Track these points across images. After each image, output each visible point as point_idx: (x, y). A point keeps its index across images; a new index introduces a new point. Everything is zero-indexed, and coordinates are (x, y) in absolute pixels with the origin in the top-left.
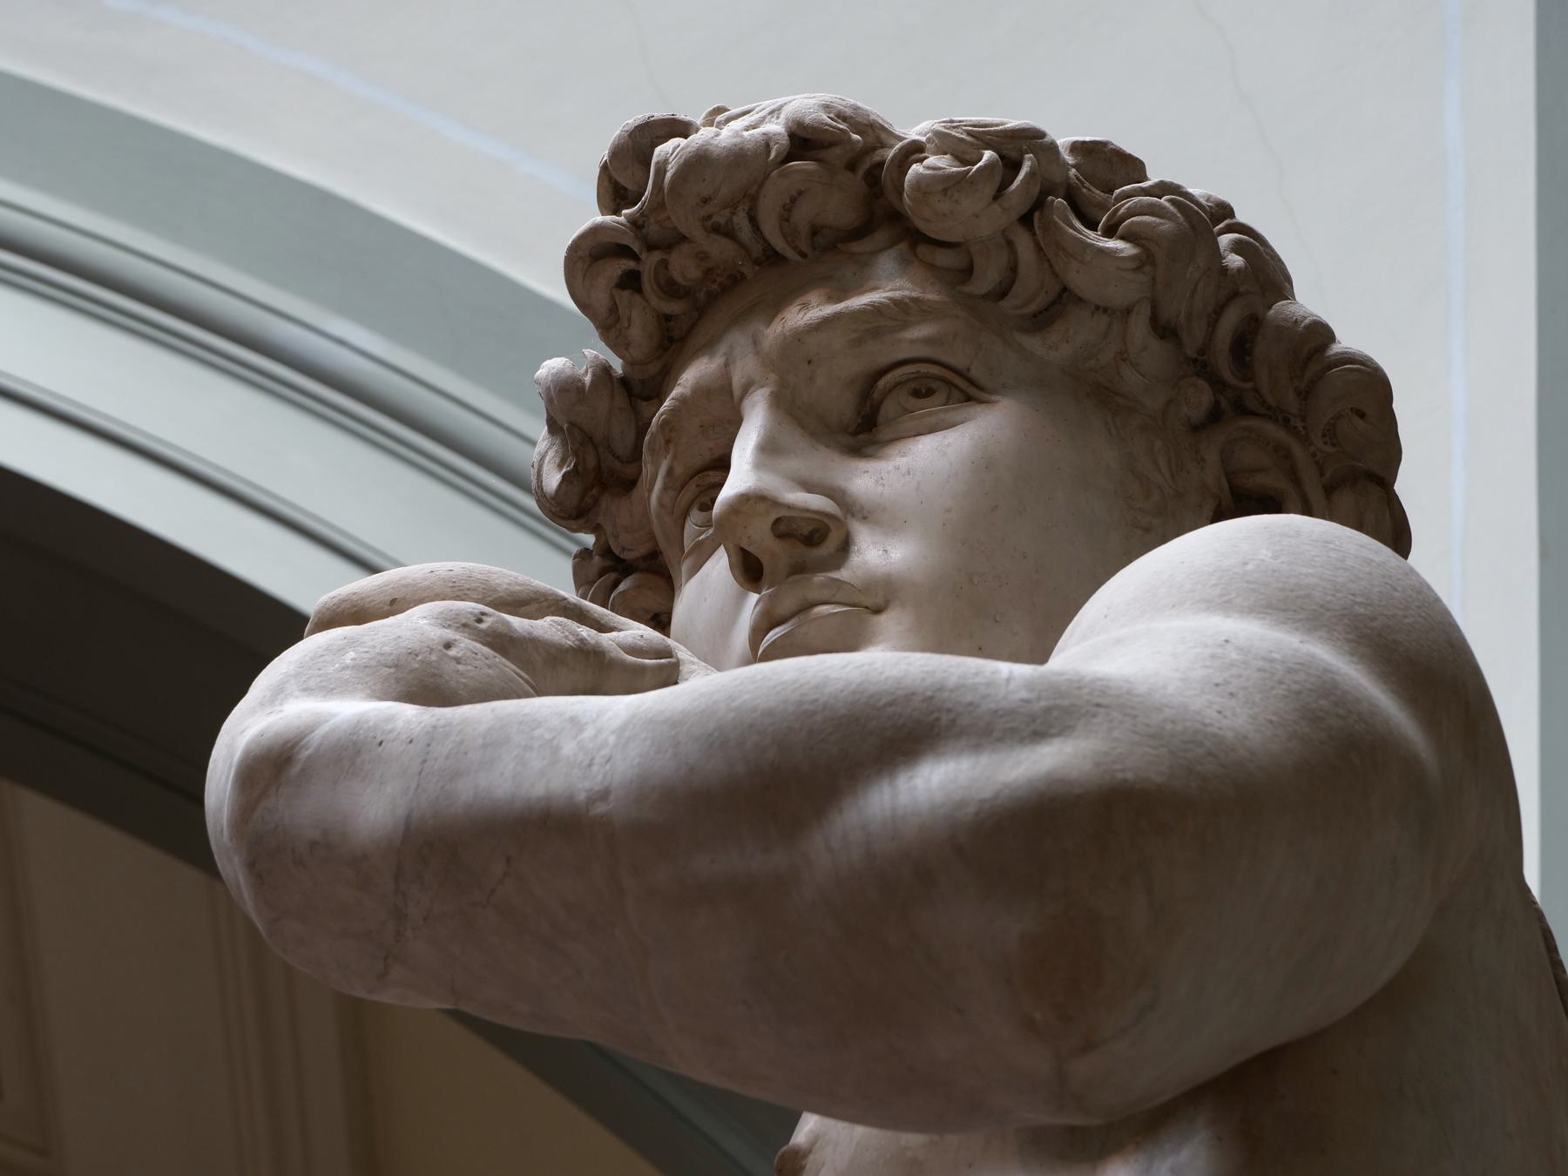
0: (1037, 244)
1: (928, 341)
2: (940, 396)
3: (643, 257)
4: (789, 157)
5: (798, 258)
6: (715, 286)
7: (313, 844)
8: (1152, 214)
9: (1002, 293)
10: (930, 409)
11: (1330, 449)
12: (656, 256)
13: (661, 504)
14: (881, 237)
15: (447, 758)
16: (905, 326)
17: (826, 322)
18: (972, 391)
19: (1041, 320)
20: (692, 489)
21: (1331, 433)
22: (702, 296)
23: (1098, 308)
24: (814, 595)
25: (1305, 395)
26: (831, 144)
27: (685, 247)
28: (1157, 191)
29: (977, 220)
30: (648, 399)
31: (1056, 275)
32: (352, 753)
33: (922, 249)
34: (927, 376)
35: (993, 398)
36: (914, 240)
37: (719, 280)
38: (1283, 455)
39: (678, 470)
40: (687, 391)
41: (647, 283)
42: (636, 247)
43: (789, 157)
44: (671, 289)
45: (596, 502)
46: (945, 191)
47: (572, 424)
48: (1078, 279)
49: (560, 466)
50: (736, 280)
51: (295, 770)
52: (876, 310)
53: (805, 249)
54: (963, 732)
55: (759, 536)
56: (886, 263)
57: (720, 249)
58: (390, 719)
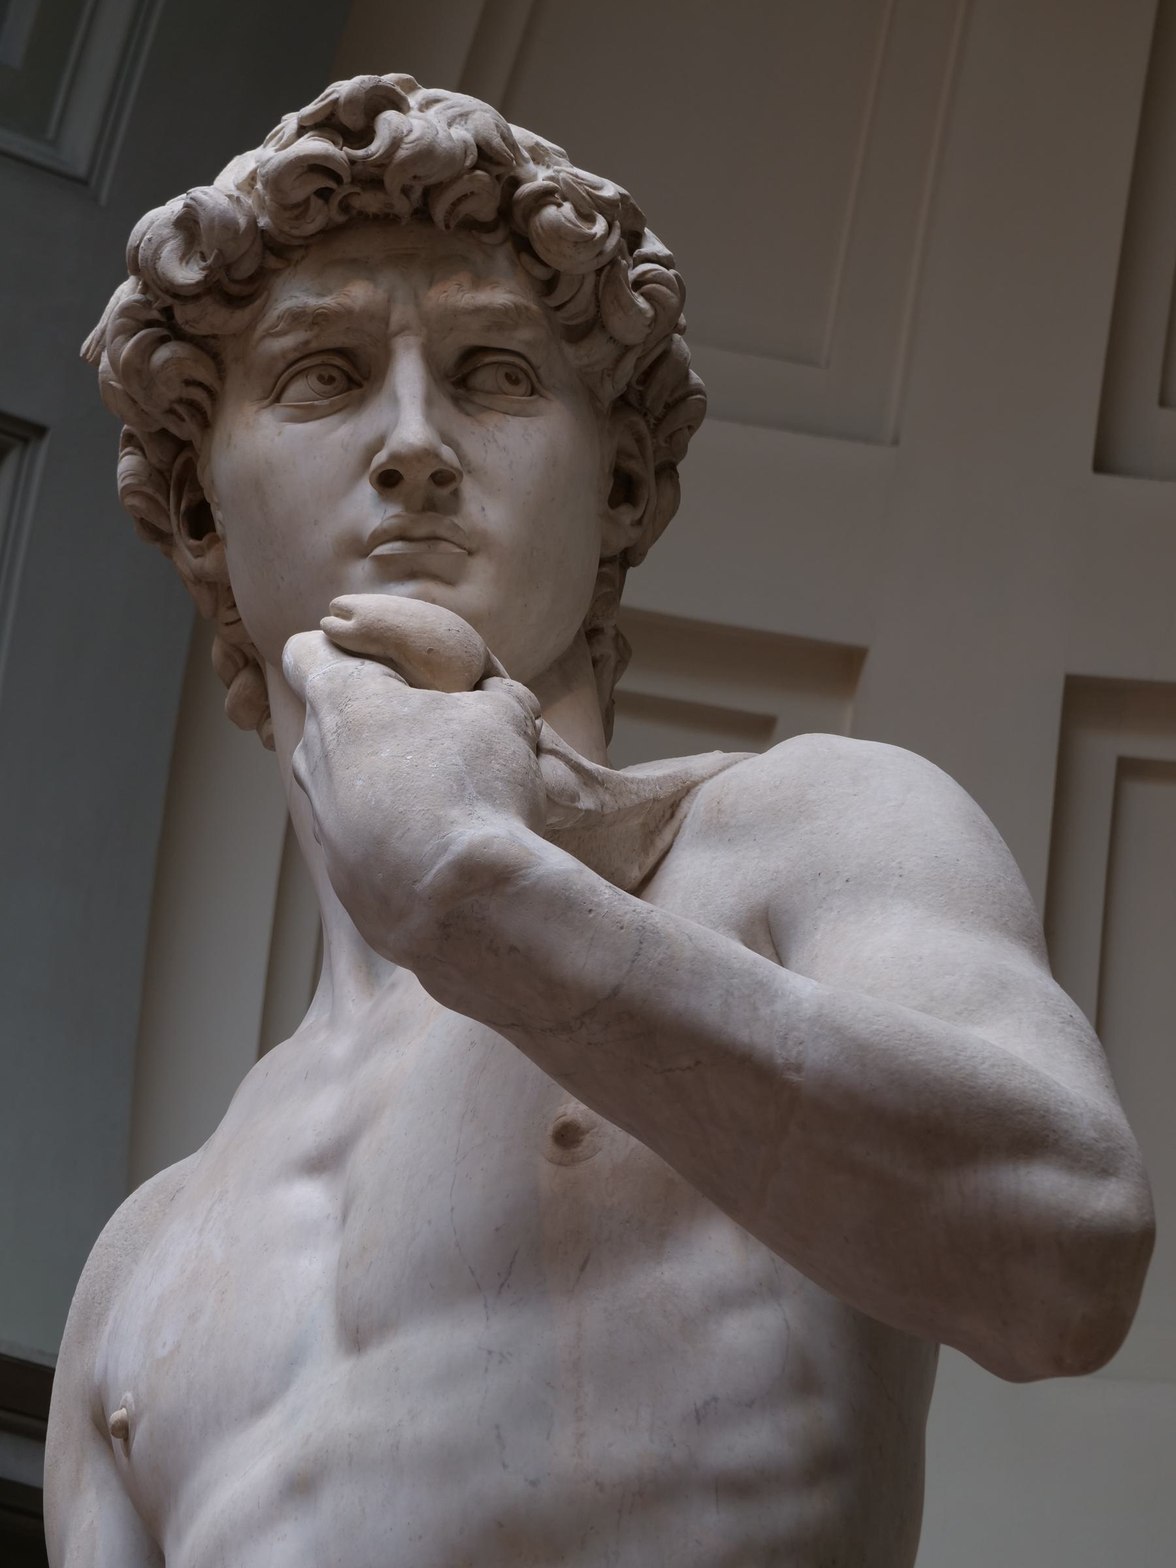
0: (596, 286)
2: (524, 387)
4: (475, 167)
5: (443, 228)
7: (513, 949)
8: (667, 287)
11: (663, 444)
12: (357, 189)
13: (284, 354)
14: (500, 234)
15: (660, 964)
17: (478, 311)
18: (537, 385)
19: (577, 334)
20: (317, 360)
21: (671, 436)
22: (354, 212)
23: (611, 338)
24: (441, 532)
25: (670, 407)
26: (499, 164)
28: (665, 261)
30: (271, 249)
31: (599, 307)
32: (562, 904)
33: (525, 258)
34: (522, 369)
36: (523, 245)
38: (639, 440)
39: (314, 346)
41: (335, 201)
42: (346, 178)
44: (345, 207)
45: (196, 297)
46: (576, 243)
47: (221, 253)
48: (617, 323)
49: (181, 259)
50: (387, 220)
52: (505, 311)
53: (453, 224)
55: (417, 477)
56: (502, 258)
57: (402, 206)
58: (593, 890)
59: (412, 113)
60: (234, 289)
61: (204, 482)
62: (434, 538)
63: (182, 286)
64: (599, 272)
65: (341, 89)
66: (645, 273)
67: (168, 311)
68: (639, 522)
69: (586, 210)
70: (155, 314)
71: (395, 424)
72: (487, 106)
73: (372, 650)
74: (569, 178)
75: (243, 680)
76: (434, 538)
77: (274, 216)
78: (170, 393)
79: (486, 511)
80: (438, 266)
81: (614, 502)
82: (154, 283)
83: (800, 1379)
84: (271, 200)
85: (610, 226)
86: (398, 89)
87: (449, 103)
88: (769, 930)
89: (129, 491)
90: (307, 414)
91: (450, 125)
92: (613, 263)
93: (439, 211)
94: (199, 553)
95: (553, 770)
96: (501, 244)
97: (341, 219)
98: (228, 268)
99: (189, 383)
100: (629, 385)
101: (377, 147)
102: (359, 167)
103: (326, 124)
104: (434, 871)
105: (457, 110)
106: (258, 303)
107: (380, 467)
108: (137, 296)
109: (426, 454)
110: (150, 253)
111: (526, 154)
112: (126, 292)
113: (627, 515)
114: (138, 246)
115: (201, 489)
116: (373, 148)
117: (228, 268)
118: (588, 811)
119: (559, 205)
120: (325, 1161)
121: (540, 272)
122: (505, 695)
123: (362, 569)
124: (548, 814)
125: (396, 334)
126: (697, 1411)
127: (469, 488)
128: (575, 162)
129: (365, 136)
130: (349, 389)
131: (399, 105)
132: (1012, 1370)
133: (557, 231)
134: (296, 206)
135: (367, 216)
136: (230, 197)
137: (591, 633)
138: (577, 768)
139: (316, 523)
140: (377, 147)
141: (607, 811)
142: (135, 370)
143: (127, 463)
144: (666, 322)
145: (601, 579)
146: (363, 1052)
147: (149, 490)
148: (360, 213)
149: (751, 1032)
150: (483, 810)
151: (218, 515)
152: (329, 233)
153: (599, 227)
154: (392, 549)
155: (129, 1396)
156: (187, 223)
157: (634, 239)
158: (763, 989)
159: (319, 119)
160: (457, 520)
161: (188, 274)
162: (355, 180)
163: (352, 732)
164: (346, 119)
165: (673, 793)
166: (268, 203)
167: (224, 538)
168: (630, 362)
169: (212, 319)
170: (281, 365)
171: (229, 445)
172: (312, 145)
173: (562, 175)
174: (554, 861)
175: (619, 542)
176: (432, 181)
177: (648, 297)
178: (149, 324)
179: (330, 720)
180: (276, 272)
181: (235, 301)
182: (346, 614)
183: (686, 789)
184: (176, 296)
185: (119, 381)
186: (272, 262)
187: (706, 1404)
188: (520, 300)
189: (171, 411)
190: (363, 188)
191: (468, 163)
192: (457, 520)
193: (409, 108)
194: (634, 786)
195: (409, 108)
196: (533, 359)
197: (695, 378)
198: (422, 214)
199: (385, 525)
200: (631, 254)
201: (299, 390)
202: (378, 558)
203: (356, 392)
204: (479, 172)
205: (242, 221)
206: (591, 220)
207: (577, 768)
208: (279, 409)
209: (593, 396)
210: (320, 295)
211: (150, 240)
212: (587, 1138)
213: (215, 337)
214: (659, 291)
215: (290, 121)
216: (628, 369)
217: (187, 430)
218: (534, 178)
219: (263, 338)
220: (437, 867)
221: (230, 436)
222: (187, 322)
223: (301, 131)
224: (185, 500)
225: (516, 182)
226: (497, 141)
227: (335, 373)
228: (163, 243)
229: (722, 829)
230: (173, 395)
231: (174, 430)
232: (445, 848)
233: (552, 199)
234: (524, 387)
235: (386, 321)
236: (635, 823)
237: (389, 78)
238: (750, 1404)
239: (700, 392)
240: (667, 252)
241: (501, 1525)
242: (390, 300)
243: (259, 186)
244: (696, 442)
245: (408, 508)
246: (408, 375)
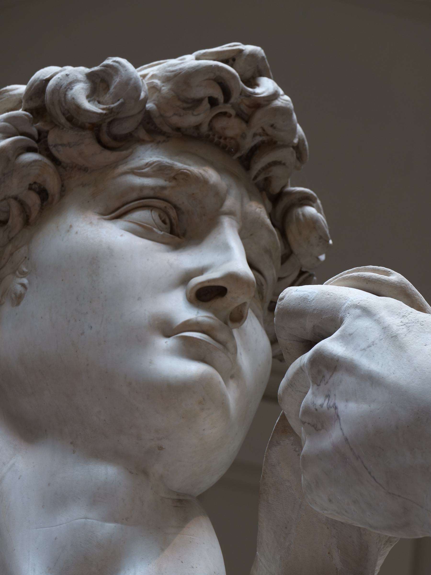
3: (229, 105)
5: (253, 177)
6: (216, 139)
12: (232, 112)
13: (142, 188)
27: (244, 125)
37: (222, 141)
39: (166, 193)
42: (232, 100)
45: (82, 127)
46: (321, 238)
49: (88, 97)
60: (106, 138)
70: (34, 130)
71: (229, 260)
78: (16, 186)
84: (171, 89)
90: (144, 232)
99: (30, 188)
106: (124, 153)
110: (65, 83)
114: (48, 80)
123: (165, 343)
133: (313, 222)
134: (185, 101)
139: (139, 299)
154: (201, 337)
170: (134, 195)
171: (68, 231)
180: (142, 142)
186: (142, 134)
203: (177, 238)
205: (143, 95)
208: (121, 223)
211: (67, 75)
221: (71, 226)
222: (55, 146)
227: (167, 221)
228: (76, 81)
233: (311, 203)
235: (222, 201)
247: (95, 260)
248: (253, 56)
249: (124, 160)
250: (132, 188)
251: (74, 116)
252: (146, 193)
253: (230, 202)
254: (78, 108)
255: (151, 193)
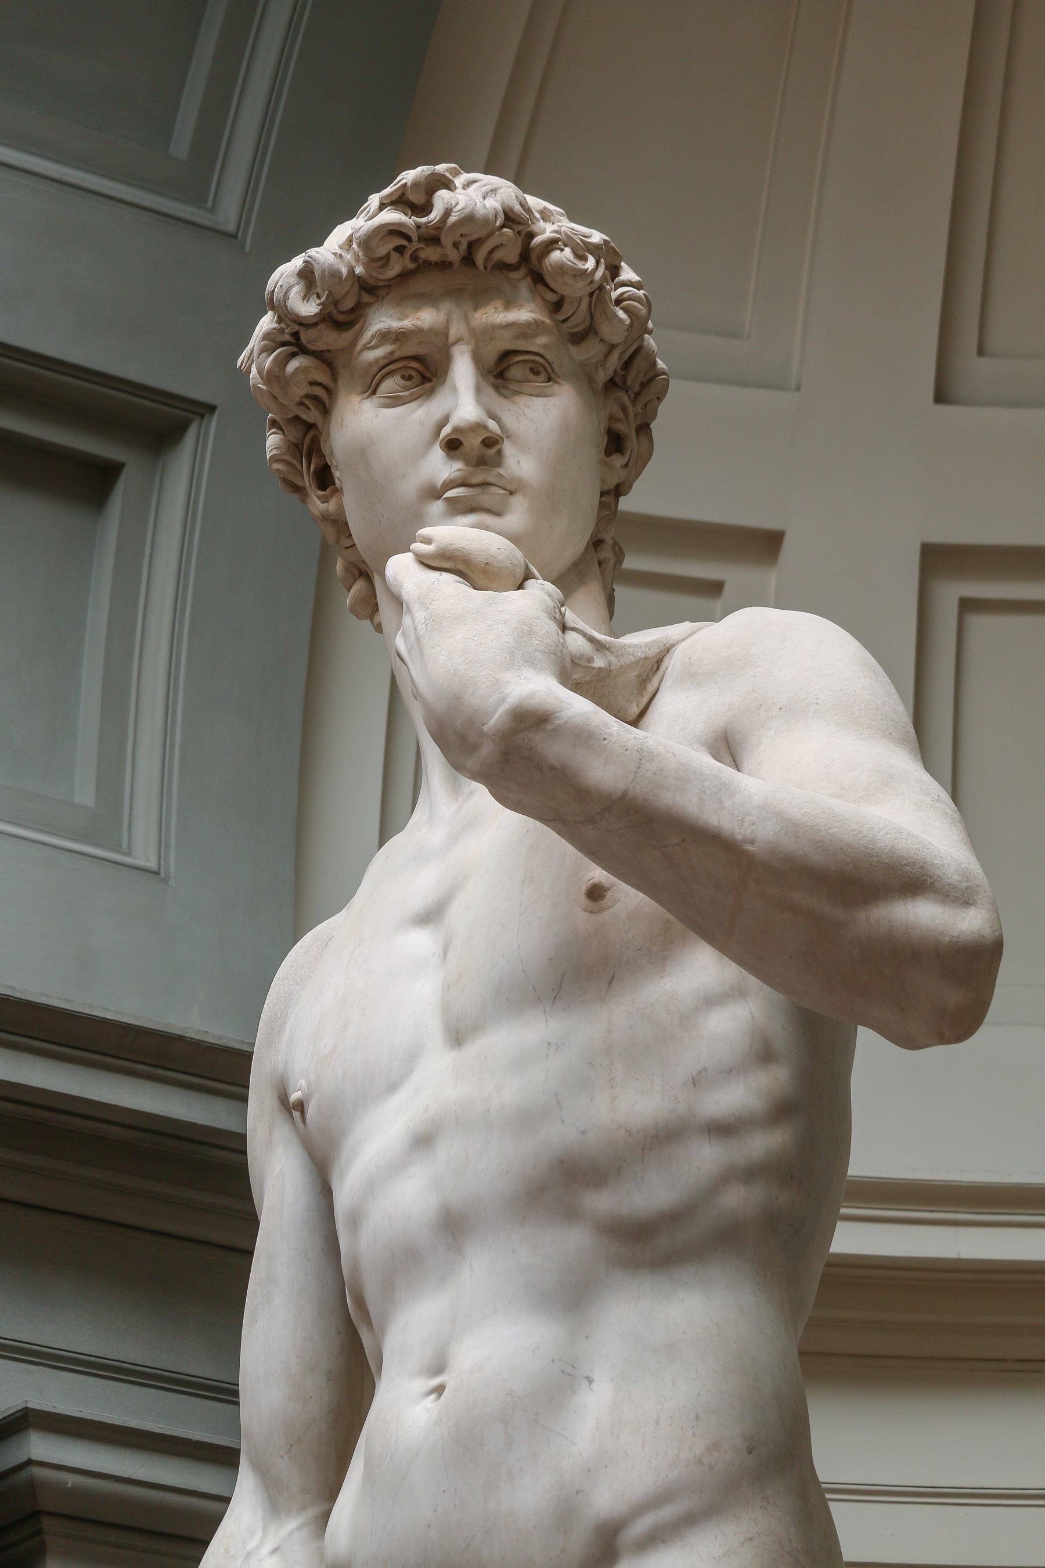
0: (590, 304)
1: (545, 346)
2: (543, 376)
4: (503, 226)
7: (552, 768)
8: (639, 302)
9: (564, 321)
10: (539, 384)
11: (640, 411)
12: (422, 245)
13: (377, 361)
14: (522, 272)
16: (535, 336)
17: (509, 325)
18: (553, 375)
19: (577, 339)
24: (491, 479)
25: (645, 385)
26: (519, 223)
27: (439, 250)
29: (577, 290)
32: (584, 736)
33: (540, 287)
34: (541, 364)
35: (562, 382)
36: (538, 279)
38: (624, 409)
39: (398, 355)
40: (426, 328)
41: (408, 254)
42: (415, 238)
43: (503, 226)
44: (414, 258)
45: (315, 324)
46: (574, 276)
47: (330, 292)
48: (605, 330)
49: (304, 299)
51: (549, 727)
52: (528, 324)
54: (936, 891)
55: (473, 443)
56: (524, 288)
57: (454, 256)
58: (606, 725)
59: (459, 190)
60: (340, 318)
61: (326, 452)
62: (485, 484)
63: (305, 317)
64: (591, 294)
65: (409, 176)
66: (623, 293)
67: (296, 335)
68: (626, 465)
69: (580, 253)
70: (287, 337)
72: (509, 183)
73: (447, 565)
74: (568, 231)
75: (359, 586)
76: (485, 484)
77: (365, 266)
78: (300, 390)
79: (521, 463)
80: (480, 297)
81: (608, 453)
82: (285, 316)
83: (764, 1054)
85: (598, 263)
86: (448, 175)
87: (483, 183)
88: (727, 746)
89: (275, 459)
90: (394, 402)
91: (484, 198)
92: (601, 288)
93: (480, 257)
94: (325, 500)
95: (575, 642)
96: (523, 278)
97: (412, 266)
98: (336, 303)
99: (313, 383)
100: (615, 371)
101: (435, 215)
102: (423, 230)
103: (400, 201)
104: (496, 717)
105: (489, 187)
106: (358, 326)
107: (446, 436)
108: (275, 325)
109: (478, 427)
111: (538, 216)
112: (267, 322)
113: (618, 461)
115: (324, 456)
116: (432, 216)
117: (336, 303)
118: (600, 669)
119: (562, 250)
120: (430, 916)
121: (551, 297)
122: (540, 591)
123: (437, 507)
124: (575, 674)
125: (454, 344)
126: (693, 1078)
127: (508, 449)
128: (571, 219)
129: (425, 208)
130: (422, 384)
131: (448, 185)
132: (909, 1043)
133: (561, 269)
134: (380, 259)
135: (430, 263)
136: (335, 254)
137: (596, 543)
138: (591, 639)
139: (404, 476)
140: (435, 215)
141: (613, 668)
142: (274, 377)
143: (273, 441)
144: (638, 326)
145: (602, 506)
146: (453, 839)
147: (289, 458)
148: (425, 261)
149: (719, 817)
150: (528, 673)
151: (337, 474)
152: (404, 276)
153: (590, 263)
155: (303, 1082)
156: (307, 274)
157: (614, 271)
158: (725, 788)
159: (394, 198)
160: (500, 471)
161: (309, 309)
162: (421, 239)
163: (436, 622)
164: (412, 197)
165: (658, 653)
166: (361, 257)
167: (341, 488)
168: (615, 355)
169: (327, 339)
170: (375, 369)
172: (391, 216)
173: (563, 229)
174: (578, 707)
175: (613, 481)
176: (474, 237)
177: (626, 310)
178: (284, 344)
179: (420, 615)
180: (369, 305)
181: (341, 326)
182: (428, 541)
183: (667, 650)
184: (301, 324)
185: (264, 384)
186: (366, 298)
187: (699, 1072)
188: (538, 316)
189: (301, 403)
190: (427, 245)
191: (498, 224)
192: (501, 471)
193: (456, 188)
194: (631, 650)
195: (456, 188)
196: (548, 357)
197: (661, 364)
198: (468, 260)
199: (453, 476)
200: (613, 281)
201: (389, 385)
202: (446, 499)
203: (427, 385)
204: (505, 230)
205: (344, 271)
206: (584, 259)
207: (591, 639)
208: (375, 399)
209: (591, 380)
210: (401, 319)
212: (609, 895)
213: (329, 351)
214: (634, 306)
215: (374, 200)
216: (614, 361)
217: (312, 416)
218: (544, 232)
219: (362, 351)
220: (498, 713)
223: (382, 206)
224: (313, 462)
225: (531, 235)
226: (517, 208)
227: (414, 373)
229: (692, 676)
230: (302, 393)
231: (304, 416)
232: (503, 700)
234: (543, 376)
235: (446, 335)
236: (633, 674)
237: (441, 168)
238: (729, 1072)
239: (664, 373)
240: (639, 279)
241: (562, 1162)
242: (448, 321)
243: (355, 246)
244: (662, 408)
245: (467, 463)
246: (463, 371)
247: (363, 453)
248: (416, 184)
249: (361, 333)
250: (370, 365)
251: (302, 322)
252: (382, 363)
253: (456, 329)
254: (298, 316)
255: (386, 361)
